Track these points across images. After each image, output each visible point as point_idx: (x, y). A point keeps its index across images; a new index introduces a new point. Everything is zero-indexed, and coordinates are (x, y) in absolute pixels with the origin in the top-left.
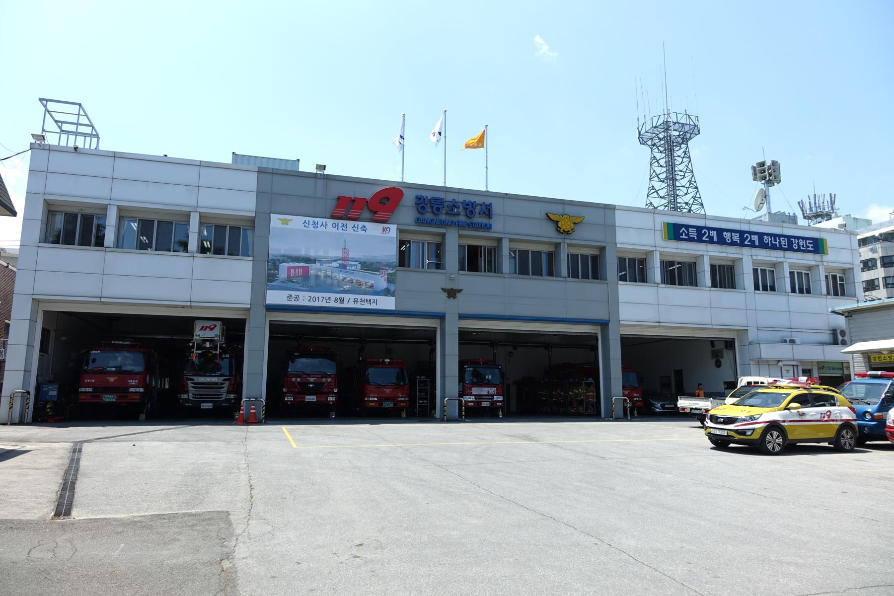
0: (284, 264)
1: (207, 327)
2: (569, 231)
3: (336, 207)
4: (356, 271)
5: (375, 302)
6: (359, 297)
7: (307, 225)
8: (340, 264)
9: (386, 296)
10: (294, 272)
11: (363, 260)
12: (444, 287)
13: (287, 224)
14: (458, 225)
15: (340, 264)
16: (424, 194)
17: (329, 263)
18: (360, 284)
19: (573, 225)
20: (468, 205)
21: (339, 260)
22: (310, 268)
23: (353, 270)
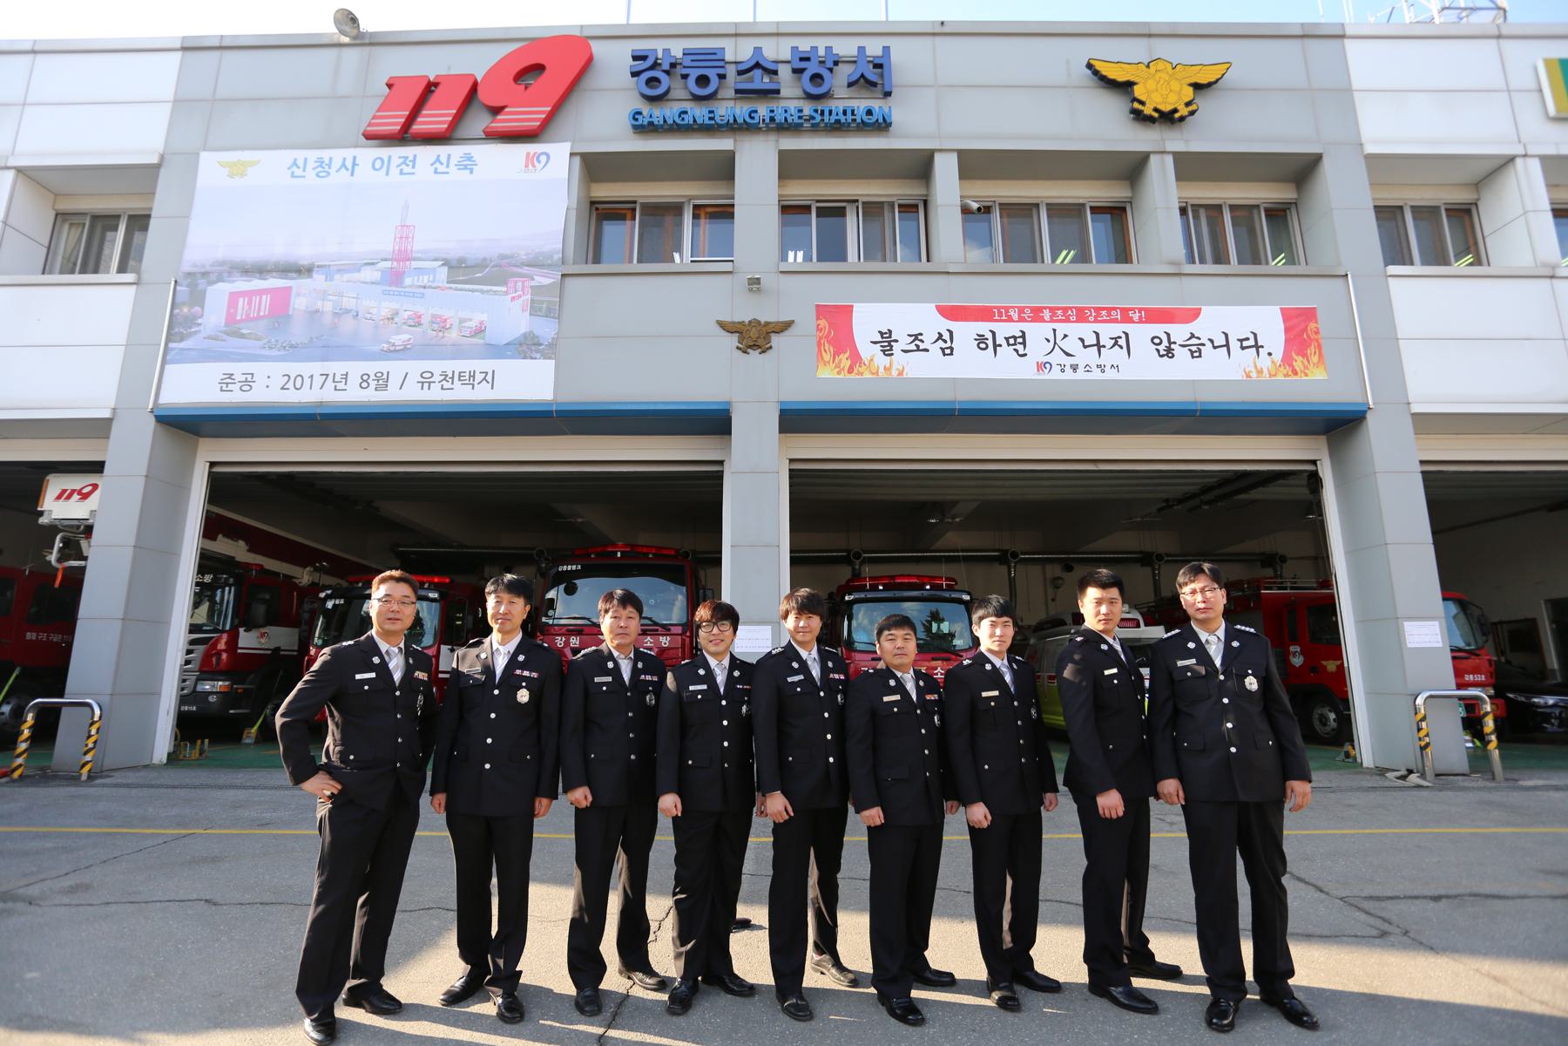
0: (220, 285)
1: (73, 491)
2: (1175, 111)
3: (378, 111)
4: (430, 287)
5: (489, 379)
6: (437, 367)
7: (298, 172)
8: (383, 272)
9: (525, 358)
10: (246, 307)
11: (455, 253)
12: (727, 318)
13: (243, 175)
14: (772, 119)
15: (383, 272)
16: (659, 46)
18: (441, 325)
19: (1189, 93)
20: (808, 59)
21: (386, 260)
22: (294, 290)
23: (425, 287)
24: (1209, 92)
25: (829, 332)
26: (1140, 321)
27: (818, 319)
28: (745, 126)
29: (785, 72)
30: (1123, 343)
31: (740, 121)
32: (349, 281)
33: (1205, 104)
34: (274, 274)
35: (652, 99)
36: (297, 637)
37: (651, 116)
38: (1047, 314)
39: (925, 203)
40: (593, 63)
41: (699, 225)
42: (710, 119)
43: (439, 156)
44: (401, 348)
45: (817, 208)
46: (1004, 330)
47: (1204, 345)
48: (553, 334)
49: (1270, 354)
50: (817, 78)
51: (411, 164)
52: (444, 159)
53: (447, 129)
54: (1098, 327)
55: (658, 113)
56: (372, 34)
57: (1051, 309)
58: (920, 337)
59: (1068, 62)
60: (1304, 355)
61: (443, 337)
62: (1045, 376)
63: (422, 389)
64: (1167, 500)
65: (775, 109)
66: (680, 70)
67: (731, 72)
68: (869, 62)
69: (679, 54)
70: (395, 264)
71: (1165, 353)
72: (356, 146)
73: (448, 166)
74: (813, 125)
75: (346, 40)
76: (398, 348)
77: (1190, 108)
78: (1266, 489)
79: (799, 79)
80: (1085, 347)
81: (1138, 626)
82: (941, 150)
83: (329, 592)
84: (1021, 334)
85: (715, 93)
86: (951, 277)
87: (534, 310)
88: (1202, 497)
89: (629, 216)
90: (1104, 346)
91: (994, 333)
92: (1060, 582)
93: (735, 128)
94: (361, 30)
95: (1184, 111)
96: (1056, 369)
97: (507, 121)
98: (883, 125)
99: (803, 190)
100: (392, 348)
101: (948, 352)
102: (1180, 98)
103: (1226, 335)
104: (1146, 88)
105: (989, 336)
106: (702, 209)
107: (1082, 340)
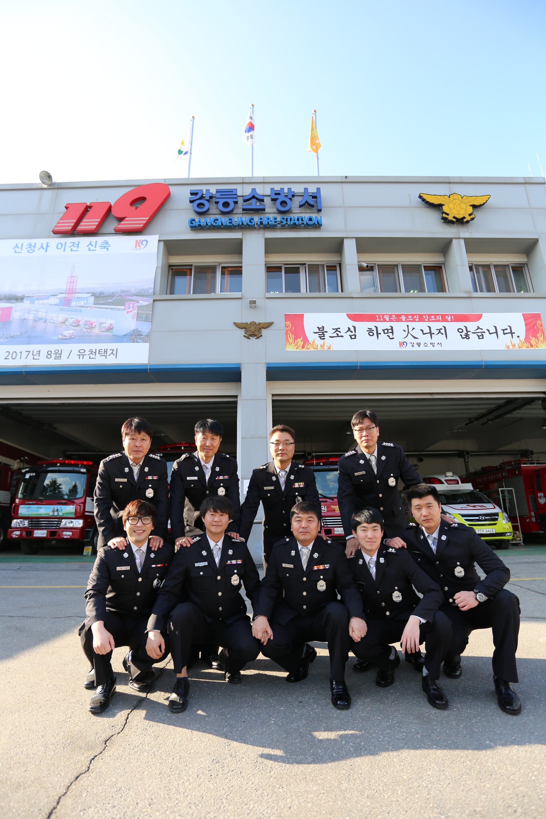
2: (464, 218)
3: (61, 219)
4: (85, 307)
5: (114, 352)
6: (87, 347)
7: (18, 250)
9: (133, 342)
12: (239, 321)
14: (261, 223)
16: (204, 188)
17: (43, 299)
18: (90, 326)
19: (470, 210)
20: (279, 194)
21: (62, 293)
22: (13, 310)
23: (82, 307)
24: (479, 209)
25: (292, 328)
26: (452, 321)
27: (286, 321)
28: (247, 226)
29: (267, 201)
30: (443, 332)
31: (245, 224)
32: (42, 304)
33: (479, 215)
34: (4, 301)
35: (200, 214)
36: (9, 497)
37: (200, 222)
38: (403, 318)
39: (340, 265)
40: (170, 196)
41: (224, 279)
42: (230, 223)
43: (91, 242)
44: (69, 337)
45: (285, 268)
46: (382, 326)
47: (484, 332)
48: (148, 330)
49: (518, 337)
50: (283, 203)
51: (76, 246)
52: (93, 244)
53: (96, 228)
54: (430, 324)
55: (203, 220)
56: (59, 184)
57: (406, 316)
58: (339, 330)
59: (409, 195)
60: (536, 337)
61: (91, 332)
62: (404, 349)
63: (79, 358)
64: (470, 419)
65: (263, 218)
66: (214, 200)
67: (240, 200)
68: (310, 195)
69: (214, 192)
70: (67, 295)
71: (465, 336)
72: (49, 237)
73: (95, 247)
74: (282, 226)
75: (45, 186)
76: (67, 338)
77: (471, 217)
78: (520, 411)
79: (275, 204)
80: (424, 334)
81: (458, 483)
82: (347, 238)
83: (27, 470)
84: (391, 328)
85: (232, 210)
86: (354, 300)
87: (139, 318)
88: (488, 417)
89: (188, 273)
90: (433, 334)
91: (377, 328)
92: (417, 467)
93: (242, 227)
94: (53, 182)
95: (468, 218)
96: (409, 345)
97: (126, 225)
98: (318, 225)
99: (278, 259)
100: (64, 338)
101: (353, 337)
102: (466, 212)
103: (496, 327)
104: (448, 207)
105: (374, 329)
106: (226, 269)
107: (422, 331)
